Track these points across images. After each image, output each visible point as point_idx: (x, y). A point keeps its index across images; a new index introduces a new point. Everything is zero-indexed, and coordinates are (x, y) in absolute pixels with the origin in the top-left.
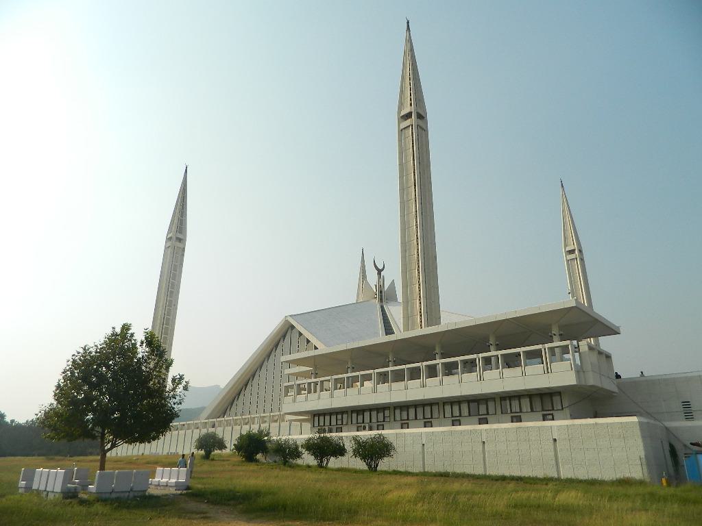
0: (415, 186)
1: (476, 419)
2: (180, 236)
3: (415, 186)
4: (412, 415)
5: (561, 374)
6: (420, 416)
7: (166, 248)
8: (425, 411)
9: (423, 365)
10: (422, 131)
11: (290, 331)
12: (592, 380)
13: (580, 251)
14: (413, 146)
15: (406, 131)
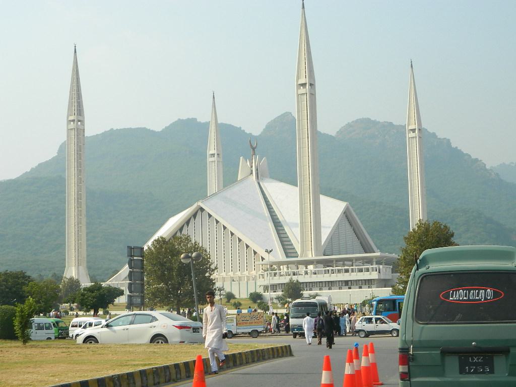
0: (308, 138)
1: (347, 287)
2: (80, 118)
3: (308, 138)
4: (324, 285)
5: (374, 275)
6: (327, 285)
7: (68, 130)
8: (330, 284)
9: (330, 268)
10: (313, 95)
11: (199, 212)
12: (382, 278)
13: (419, 129)
14: (307, 109)
15: (302, 97)
